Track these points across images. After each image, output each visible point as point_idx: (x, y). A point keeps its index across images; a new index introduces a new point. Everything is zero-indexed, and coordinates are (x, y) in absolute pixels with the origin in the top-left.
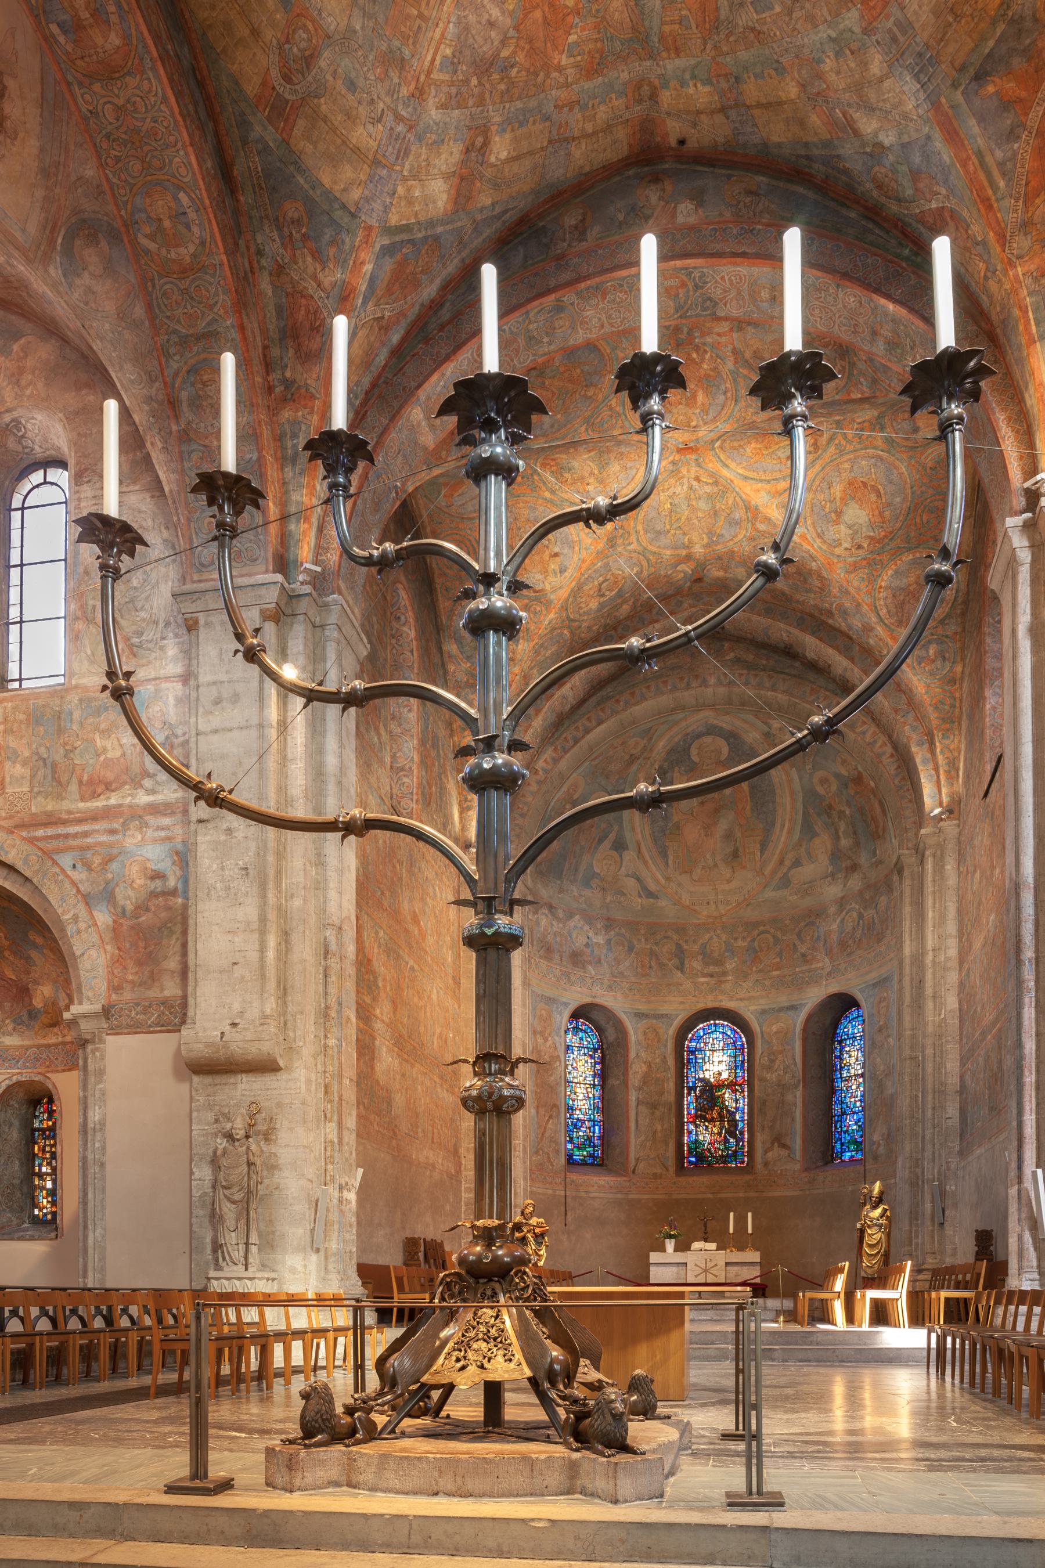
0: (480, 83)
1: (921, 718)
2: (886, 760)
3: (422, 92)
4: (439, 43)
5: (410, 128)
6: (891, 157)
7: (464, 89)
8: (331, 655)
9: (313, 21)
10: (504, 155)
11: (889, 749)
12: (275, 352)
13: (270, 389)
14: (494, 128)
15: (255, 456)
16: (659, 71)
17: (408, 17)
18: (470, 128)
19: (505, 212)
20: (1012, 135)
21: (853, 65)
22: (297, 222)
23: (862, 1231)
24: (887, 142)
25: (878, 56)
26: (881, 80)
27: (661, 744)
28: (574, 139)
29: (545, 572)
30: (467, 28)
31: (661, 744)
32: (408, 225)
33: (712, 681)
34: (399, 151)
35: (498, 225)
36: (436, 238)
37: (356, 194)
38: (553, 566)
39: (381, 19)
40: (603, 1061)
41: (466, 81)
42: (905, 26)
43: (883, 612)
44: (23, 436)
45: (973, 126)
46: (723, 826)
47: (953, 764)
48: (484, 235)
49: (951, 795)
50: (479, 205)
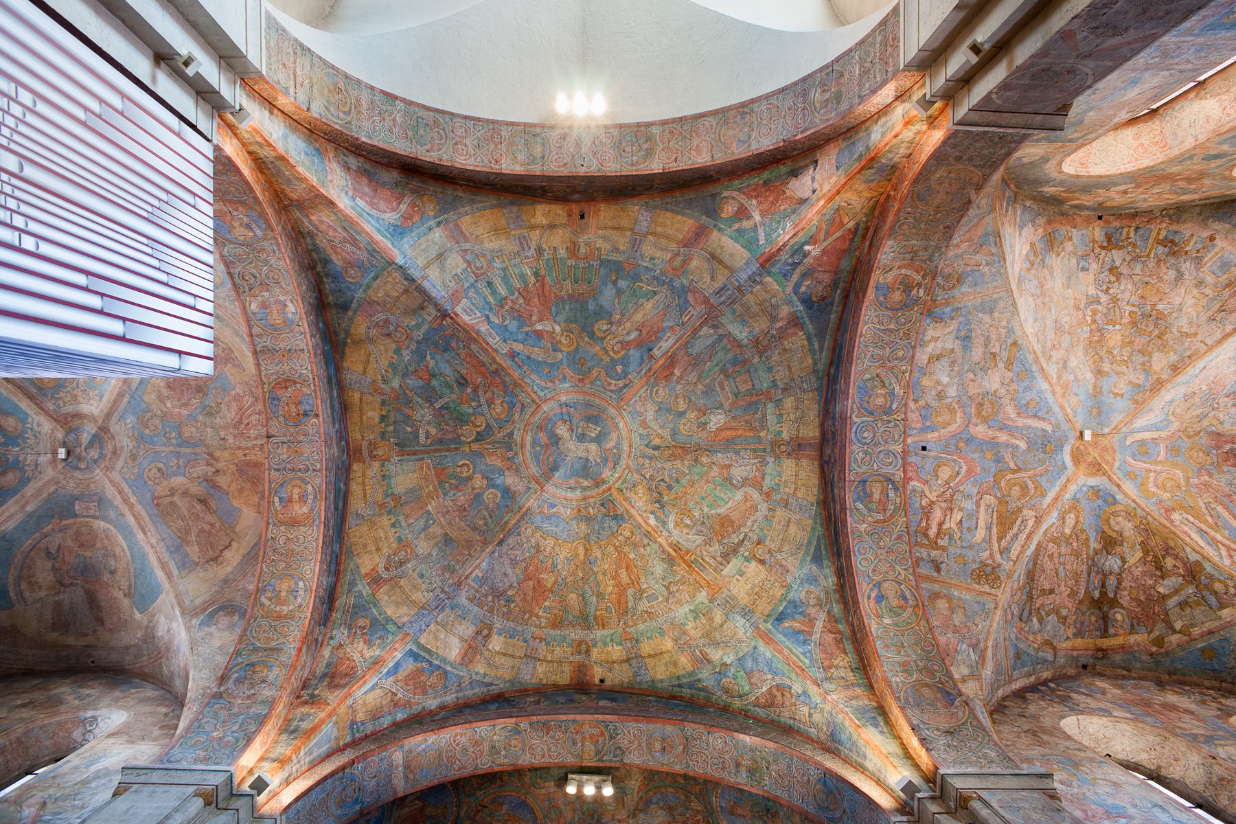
0: (493, 601)
3: (460, 584)
4: (477, 567)
5: (448, 598)
6: (732, 670)
7: (483, 599)
9: (411, 549)
10: (497, 648)
14: (495, 630)
16: (593, 636)
17: (463, 554)
18: (482, 621)
19: (491, 684)
21: (704, 622)
24: (729, 662)
25: (719, 612)
26: (722, 625)
28: (539, 660)
30: (492, 570)
32: (430, 651)
34: (439, 605)
35: (485, 690)
36: (445, 672)
39: (448, 553)
41: (486, 596)
42: (733, 598)
44: (90, 731)
48: (475, 691)
50: (476, 670)
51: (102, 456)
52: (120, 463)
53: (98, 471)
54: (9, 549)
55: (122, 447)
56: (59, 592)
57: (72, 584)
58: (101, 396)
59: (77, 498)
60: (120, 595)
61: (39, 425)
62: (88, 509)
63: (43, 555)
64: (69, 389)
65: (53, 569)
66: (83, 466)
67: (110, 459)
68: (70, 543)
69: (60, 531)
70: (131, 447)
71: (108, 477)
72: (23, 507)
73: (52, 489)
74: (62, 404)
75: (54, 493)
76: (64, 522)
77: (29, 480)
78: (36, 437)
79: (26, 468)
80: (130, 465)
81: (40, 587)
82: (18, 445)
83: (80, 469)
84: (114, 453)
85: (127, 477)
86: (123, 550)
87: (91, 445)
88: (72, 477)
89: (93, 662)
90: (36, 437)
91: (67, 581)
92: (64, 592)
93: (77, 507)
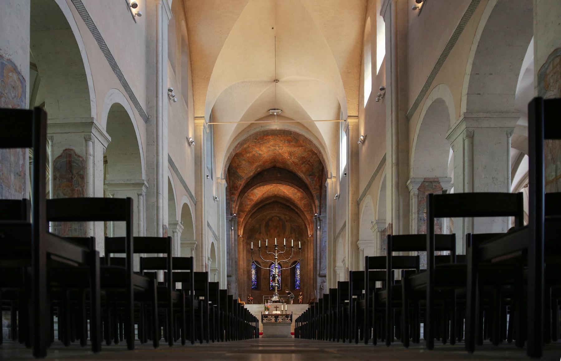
1: (308, 220)
2: (303, 225)
8: (236, 225)
11: (304, 224)
12: (231, 189)
13: (230, 193)
15: (229, 201)
20: (313, 181)
22: (236, 177)
23: (299, 299)
27: (268, 217)
29: (253, 197)
31: (268, 217)
33: (277, 210)
37: (243, 176)
38: (255, 196)
40: (257, 270)
43: (302, 206)
45: (309, 179)
46: (277, 231)
47: (312, 229)
49: (312, 234)
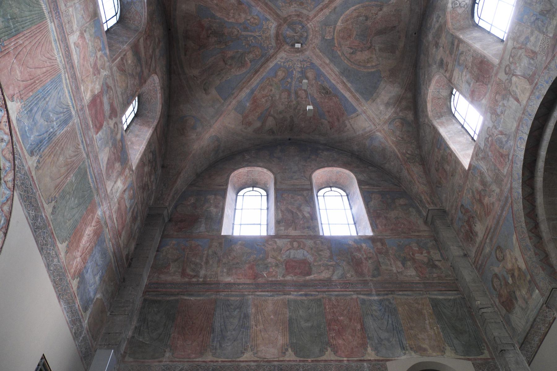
51: (300, 23)
52: (305, 12)
53: (308, 25)
54: (349, 71)
55: (295, 11)
56: (374, 49)
57: (371, 43)
58: (267, 19)
59: (323, 38)
60: (380, 13)
61: (282, 58)
62: (329, 32)
63: (353, 56)
64: (262, 42)
65: (361, 51)
66: (305, 34)
67: (302, 18)
68: (348, 42)
69: (341, 47)
70: (296, 5)
71: (313, 19)
72: (327, 64)
73: (317, 50)
74: (270, 45)
75: (319, 49)
76: (336, 45)
77: (312, 63)
78: (289, 61)
79: (305, 66)
80: (306, 5)
81: (371, 58)
82: (292, 71)
83: (307, 36)
84: (298, 16)
85: (313, 6)
86: (355, 10)
87: (294, 30)
88: (311, 40)
89: (415, 34)
90: (289, 61)
91: (369, 45)
92: (375, 46)
93: (328, 38)
